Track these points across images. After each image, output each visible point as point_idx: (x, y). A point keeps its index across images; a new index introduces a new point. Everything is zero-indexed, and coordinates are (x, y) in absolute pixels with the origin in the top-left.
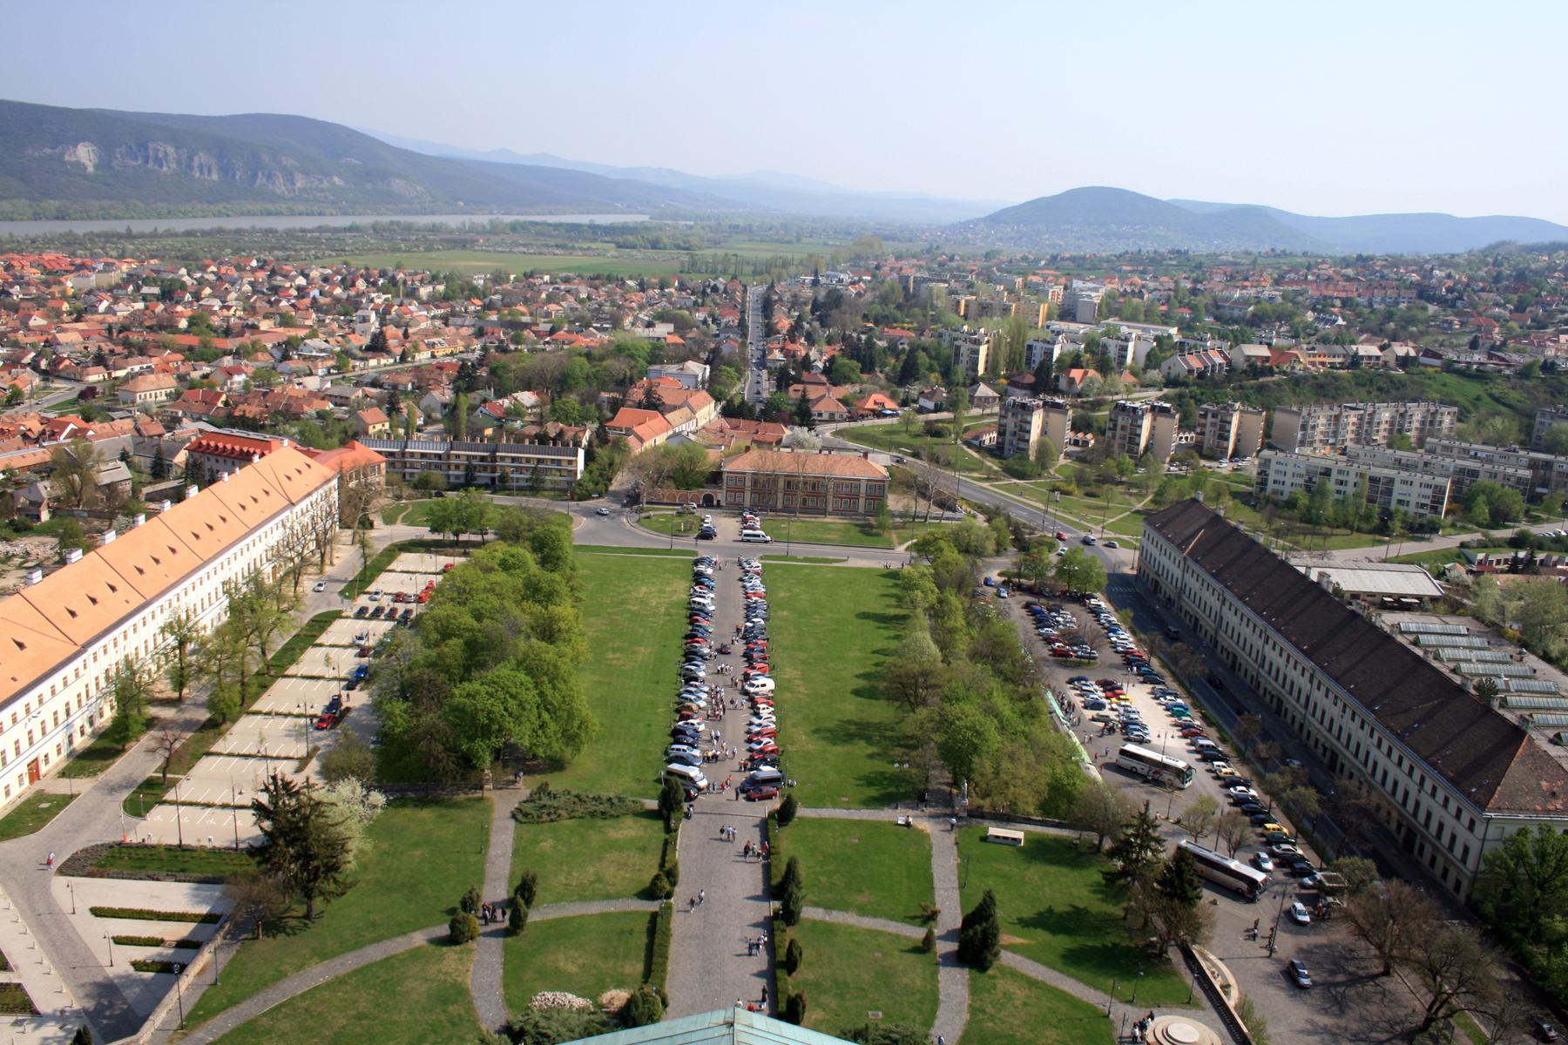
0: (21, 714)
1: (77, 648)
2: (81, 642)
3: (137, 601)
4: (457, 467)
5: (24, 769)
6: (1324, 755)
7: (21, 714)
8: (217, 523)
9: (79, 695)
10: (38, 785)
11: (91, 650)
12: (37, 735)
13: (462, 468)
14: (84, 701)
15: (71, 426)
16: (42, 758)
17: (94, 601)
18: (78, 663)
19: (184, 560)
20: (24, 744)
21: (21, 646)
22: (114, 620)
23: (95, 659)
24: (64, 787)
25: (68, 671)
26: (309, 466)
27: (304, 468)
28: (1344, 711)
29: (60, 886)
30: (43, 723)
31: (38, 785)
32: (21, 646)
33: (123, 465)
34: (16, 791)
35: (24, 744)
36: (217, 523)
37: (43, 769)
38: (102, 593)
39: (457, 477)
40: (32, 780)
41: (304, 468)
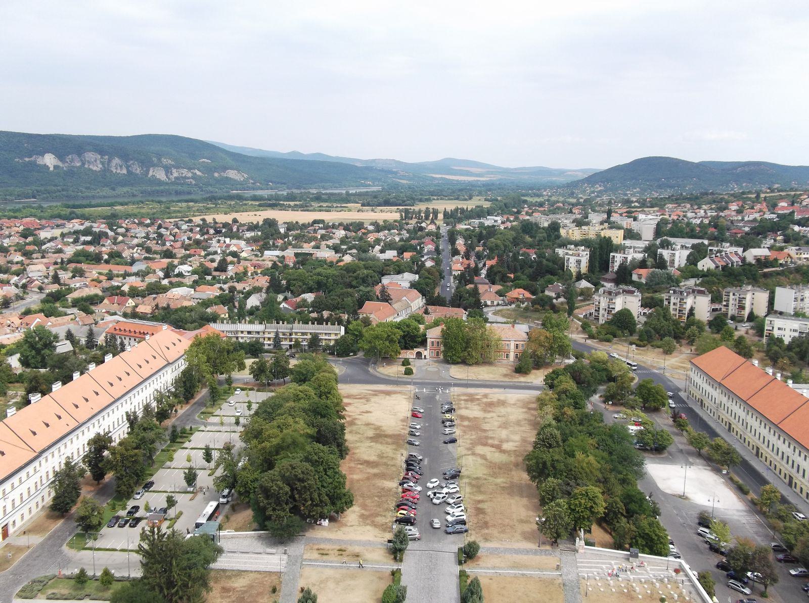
1: (36, 454)
2: (38, 450)
3: (73, 424)
4: (269, 339)
6: (785, 478)
11: (44, 455)
13: (272, 340)
14: (39, 487)
15: (38, 320)
16: (11, 523)
17: (47, 425)
18: (36, 463)
19: (105, 400)
25: (30, 469)
26: (180, 341)
27: (177, 342)
28: (794, 451)
31: (8, 540)
33: (68, 342)
37: (11, 530)
38: (53, 420)
39: (269, 345)
41: (177, 342)
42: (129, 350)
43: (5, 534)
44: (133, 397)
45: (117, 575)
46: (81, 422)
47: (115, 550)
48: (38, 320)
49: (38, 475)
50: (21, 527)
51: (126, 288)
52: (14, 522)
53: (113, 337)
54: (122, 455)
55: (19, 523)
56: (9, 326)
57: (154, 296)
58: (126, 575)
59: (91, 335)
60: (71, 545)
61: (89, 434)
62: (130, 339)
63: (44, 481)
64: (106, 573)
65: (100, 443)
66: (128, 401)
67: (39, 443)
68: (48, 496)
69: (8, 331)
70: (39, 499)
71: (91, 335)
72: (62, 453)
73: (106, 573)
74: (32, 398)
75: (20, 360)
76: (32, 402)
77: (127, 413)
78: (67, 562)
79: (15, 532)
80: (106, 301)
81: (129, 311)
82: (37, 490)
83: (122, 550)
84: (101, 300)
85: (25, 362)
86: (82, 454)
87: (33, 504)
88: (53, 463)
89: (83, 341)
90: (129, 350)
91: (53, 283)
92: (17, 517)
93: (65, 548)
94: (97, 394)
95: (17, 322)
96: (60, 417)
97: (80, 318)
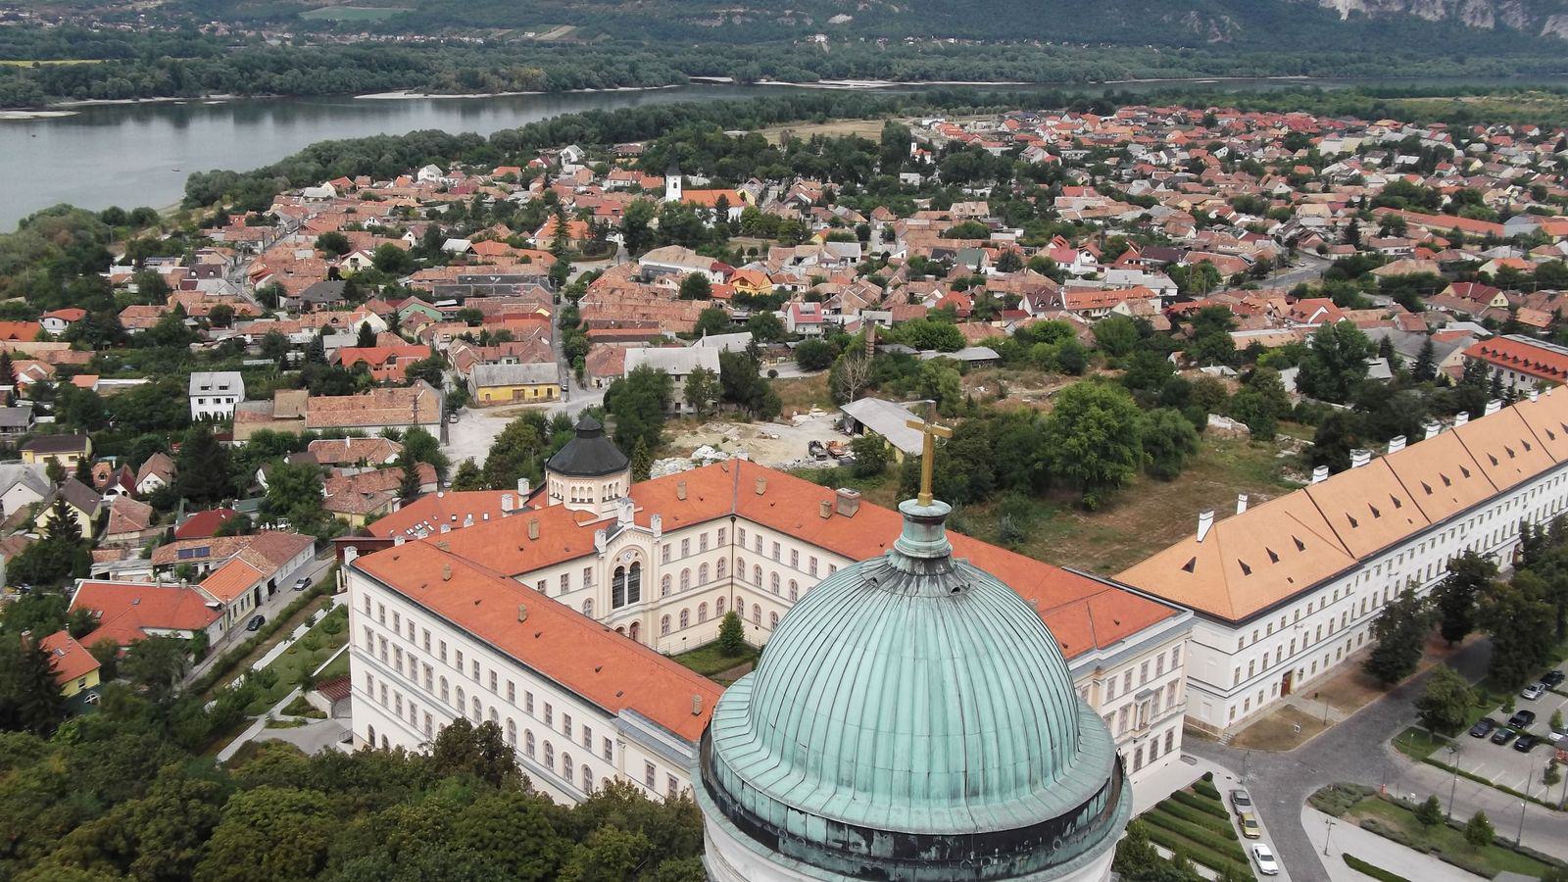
0: (1290, 620)
1: (1353, 562)
3: (1420, 523)
5: (1279, 678)
7: (1290, 620)
8: (1519, 450)
9: (1345, 614)
10: (1288, 700)
11: (1368, 566)
12: (1299, 646)
14: (1347, 623)
15: (1323, 310)
16: (1297, 671)
17: (1376, 513)
18: (1351, 579)
20: (1285, 654)
21: (1301, 546)
22: (1394, 539)
23: (1367, 578)
24: (1316, 709)
25: (1340, 586)
29: (1312, 820)
30: (1307, 634)
31: (1288, 700)
32: (1301, 546)
33: (1383, 361)
34: (1268, 699)
35: (1285, 654)
36: (1519, 450)
37: (1295, 684)
38: (1386, 507)
40: (1282, 695)
42: (1533, 399)
43: (1286, 688)
44: (1529, 495)
45: (1498, 833)
46: (1434, 521)
47: (1487, 783)
48: (1323, 310)
49: (1350, 600)
50: (1309, 684)
51: (1491, 269)
52: (1302, 671)
53: (1482, 367)
54: (1517, 605)
55: (1308, 677)
56: (1270, 313)
57: (1552, 292)
58: (1512, 838)
59: (1427, 355)
60: (1401, 744)
61: (1447, 547)
62: (1512, 375)
63: (1357, 615)
64: (1479, 821)
65: (1470, 571)
66: (1521, 500)
67: (1363, 542)
68: (1361, 640)
69: (1269, 323)
70: (1343, 643)
71: (1427, 355)
72: (1393, 571)
73: (1479, 821)
74: (1355, 458)
75: (1297, 380)
76: (1354, 465)
77: (1524, 527)
78: (1393, 774)
79: (1300, 688)
80: (1449, 290)
81: (1502, 317)
82: (1343, 626)
83: (1501, 788)
84: (1441, 286)
85: (1304, 385)
86: (1436, 580)
87: (1332, 650)
88: (1376, 587)
89: (1409, 362)
90: (1533, 399)
91: (1345, 242)
92: (1307, 664)
93: (1388, 746)
94: (1466, 474)
95: (1285, 308)
96: (1398, 504)
97: (1400, 317)
